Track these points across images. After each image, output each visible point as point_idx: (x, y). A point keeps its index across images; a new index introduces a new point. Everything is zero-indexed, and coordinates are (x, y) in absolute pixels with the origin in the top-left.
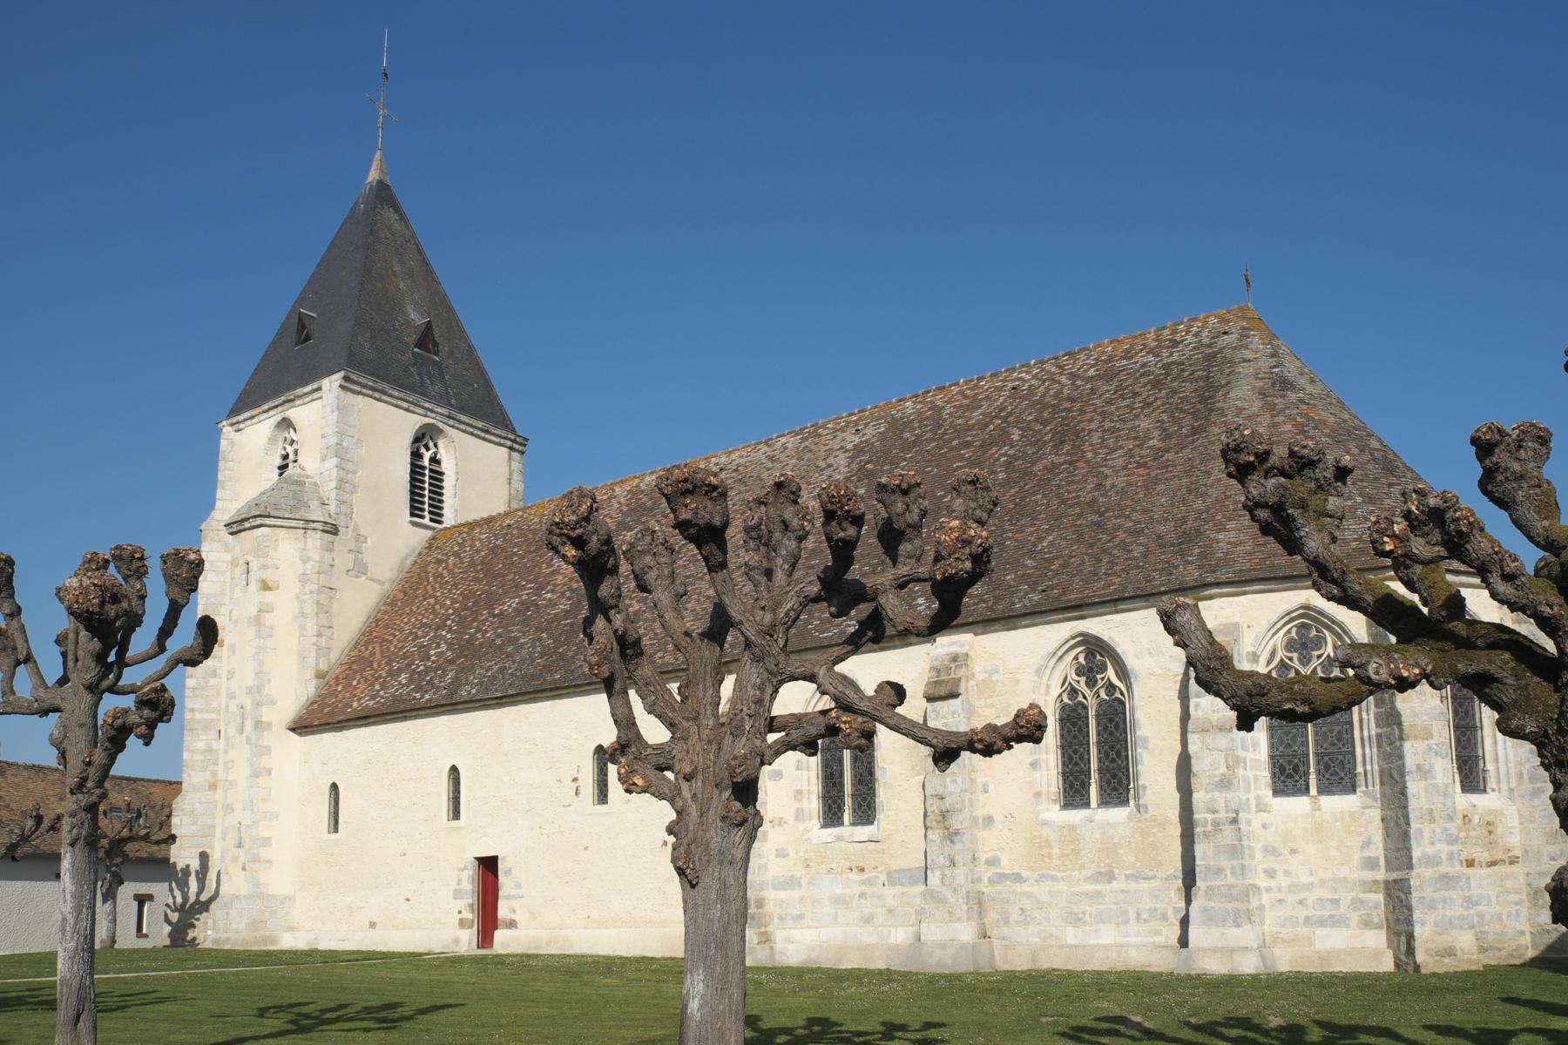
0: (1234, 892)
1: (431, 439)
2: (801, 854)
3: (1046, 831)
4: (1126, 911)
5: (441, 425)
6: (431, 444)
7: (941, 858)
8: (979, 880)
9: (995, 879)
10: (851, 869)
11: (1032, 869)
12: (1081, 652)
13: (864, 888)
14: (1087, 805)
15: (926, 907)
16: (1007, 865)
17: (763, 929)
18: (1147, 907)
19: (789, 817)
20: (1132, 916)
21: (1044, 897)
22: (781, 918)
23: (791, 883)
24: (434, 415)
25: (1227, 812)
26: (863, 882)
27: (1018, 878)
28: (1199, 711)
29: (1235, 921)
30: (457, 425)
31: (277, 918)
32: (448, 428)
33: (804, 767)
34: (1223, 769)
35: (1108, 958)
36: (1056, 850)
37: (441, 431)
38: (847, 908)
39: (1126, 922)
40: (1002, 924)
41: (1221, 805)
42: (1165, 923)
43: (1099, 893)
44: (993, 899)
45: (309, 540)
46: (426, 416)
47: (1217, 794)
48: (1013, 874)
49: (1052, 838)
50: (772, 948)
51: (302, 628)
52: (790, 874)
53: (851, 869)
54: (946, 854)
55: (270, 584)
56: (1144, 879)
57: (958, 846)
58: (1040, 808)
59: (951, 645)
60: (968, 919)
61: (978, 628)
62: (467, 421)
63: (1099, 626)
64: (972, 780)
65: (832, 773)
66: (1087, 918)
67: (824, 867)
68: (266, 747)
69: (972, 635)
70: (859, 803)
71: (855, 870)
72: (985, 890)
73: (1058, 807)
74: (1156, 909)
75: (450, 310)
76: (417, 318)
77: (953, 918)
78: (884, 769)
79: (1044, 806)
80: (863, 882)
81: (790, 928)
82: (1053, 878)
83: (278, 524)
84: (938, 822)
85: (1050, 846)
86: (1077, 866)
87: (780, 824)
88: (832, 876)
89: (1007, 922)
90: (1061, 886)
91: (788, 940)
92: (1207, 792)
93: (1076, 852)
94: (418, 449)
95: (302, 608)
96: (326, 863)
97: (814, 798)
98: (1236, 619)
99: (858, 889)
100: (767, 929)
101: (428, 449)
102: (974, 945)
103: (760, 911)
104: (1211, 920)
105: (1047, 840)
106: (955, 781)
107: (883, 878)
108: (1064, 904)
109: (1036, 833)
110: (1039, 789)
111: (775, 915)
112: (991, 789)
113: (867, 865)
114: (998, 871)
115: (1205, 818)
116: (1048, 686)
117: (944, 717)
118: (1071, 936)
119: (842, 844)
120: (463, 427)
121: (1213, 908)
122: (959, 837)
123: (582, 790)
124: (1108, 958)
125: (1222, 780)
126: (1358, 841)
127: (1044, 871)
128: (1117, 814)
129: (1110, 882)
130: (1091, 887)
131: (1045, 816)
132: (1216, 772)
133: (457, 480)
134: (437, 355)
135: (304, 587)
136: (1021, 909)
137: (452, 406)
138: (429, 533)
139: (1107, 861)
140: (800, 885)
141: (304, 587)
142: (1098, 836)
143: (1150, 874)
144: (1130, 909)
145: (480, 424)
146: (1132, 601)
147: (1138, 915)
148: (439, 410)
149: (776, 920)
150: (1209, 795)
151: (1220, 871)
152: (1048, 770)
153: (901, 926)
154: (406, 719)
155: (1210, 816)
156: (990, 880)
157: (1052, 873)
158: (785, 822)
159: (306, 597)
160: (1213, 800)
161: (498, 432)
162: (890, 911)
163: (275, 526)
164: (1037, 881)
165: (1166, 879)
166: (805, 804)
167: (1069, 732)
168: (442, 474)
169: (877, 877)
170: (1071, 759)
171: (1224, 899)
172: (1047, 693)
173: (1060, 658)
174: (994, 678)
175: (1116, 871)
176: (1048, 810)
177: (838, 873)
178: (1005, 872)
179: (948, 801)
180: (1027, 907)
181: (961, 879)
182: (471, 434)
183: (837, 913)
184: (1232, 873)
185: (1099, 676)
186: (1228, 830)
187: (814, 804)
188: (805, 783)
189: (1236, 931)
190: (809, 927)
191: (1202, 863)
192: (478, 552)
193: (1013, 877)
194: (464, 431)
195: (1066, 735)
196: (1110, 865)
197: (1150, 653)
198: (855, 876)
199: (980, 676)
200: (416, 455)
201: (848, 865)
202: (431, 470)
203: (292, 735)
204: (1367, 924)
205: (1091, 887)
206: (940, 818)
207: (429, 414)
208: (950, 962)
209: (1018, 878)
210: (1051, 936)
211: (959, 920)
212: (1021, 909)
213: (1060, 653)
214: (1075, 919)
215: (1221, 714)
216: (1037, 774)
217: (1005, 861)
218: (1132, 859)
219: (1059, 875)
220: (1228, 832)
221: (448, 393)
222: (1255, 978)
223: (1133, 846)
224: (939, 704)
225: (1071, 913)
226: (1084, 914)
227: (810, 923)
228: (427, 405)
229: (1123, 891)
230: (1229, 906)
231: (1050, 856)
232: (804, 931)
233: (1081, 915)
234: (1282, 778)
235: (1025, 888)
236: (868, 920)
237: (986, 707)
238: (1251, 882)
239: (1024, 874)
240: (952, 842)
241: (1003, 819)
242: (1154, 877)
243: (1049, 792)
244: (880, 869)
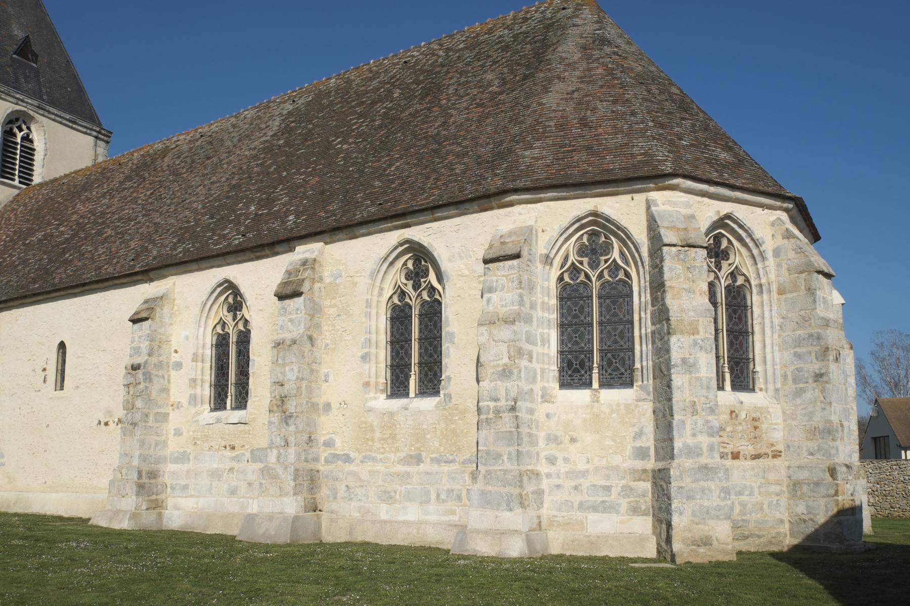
0: (509, 477)
1: (25, 123)
2: (191, 433)
3: (372, 418)
4: (429, 491)
5: (31, 113)
6: (24, 127)
7: (278, 439)
8: (316, 460)
9: (330, 459)
10: (225, 447)
11: (358, 450)
12: (409, 258)
13: (234, 464)
14: (407, 395)
15: (264, 482)
16: (340, 446)
17: (154, 497)
18: (445, 488)
19: (184, 401)
20: (433, 496)
21: (365, 476)
22: (173, 488)
23: (182, 458)
24: (25, 105)
25: (507, 400)
26: (233, 459)
27: (347, 459)
28: (490, 306)
29: (508, 505)
30: (46, 114)
32: (38, 116)
33: (200, 359)
34: (505, 360)
35: (409, 534)
36: (377, 435)
37: (32, 118)
38: (219, 480)
39: (428, 501)
40: (331, 499)
41: (502, 394)
42: (459, 504)
43: (408, 474)
44: (327, 477)
46: (17, 104)
47: (499, 383)
48: (344, 455)
49: (375, 424)
50: (160, 514)
52: (182, 450)
53: (225, 447)
54: (282, 435)
56: (446, 462)
57: (292, 428)
58: (367, 396)
59: (305, 252)
60: (295, 494)
61: (326, 237)
62: (56, 112)
63: (419, 233)
64: (312, 371)
65: (222, 365)
66: (397, 497)
69: (322, 244)
70: (219, 392)
71: (228, 448)
72: (321, 468)
73: (384, 396)
74: (452, 491)
75: (54, 34)
76: (19, 33)
77: (282, 493)
78: (254, 360)
79: (372, 395)
80: (233, 459)
81: (178, 497)
82: (374, 459)
84: (278, 406)
85: (373, 431)
86: (393, 449)
87: (178, 408)
88: (211, 452)
89: (335, 498)
90: (380, 467)
91: (176, 508)
92: (491, 381)
93: (393, 437)
94: (11, 129)
97: (207, 386)
98: (531, 223)
99: (228, 464)
100: (159, 497)
101: (21, 130)
102: (296, 519)
103: (152, 481)
104: (488, 503)
105: (371, 426)
106: (292, 369)
107: (248, 455)
108: (380, 483)
109: (363, 419)
110: (367, 380)
111: (169, 486)
112: (331, 378)
113: (237, 443)
114: (333, 452)
115: (488, 406)
116: (381, 289)
118: (384, 512)
119: (220, 425)
120: (53, 117)
121: (490, 492)
122: (292, 420)
123: (48, 379)
124: (409, 534)
125: (504, 370)
126: (631, 432)
127: (368, 453)
128: (429, 403)
129: (418, 465)
130: (402, 469)
131: (372, 404)
132: (500, 362)
133: (45, 155)
134: (36, 63)
136: (347, 486)
137: (44, 100)
138: (17, 192)
139: (416, 446)
140: (189, 460)
142: (410, 422)
143: (451, 458)
144: (431, 489)
145: (68, 116)
147: (438, 495)
148: (30, 101)
149: (169, 489)
150: (493, 384)
151: (498, 456)
152: (377, 363)
155: (492, 404)
156: (327, 461)
157: (373, 455)
158: (182, 406)
160: (496, 389)
161: (84, 124)
162: (250, 484)
164: (362, 462)
165: (463, 463)
166: (198, 391)
167: (398, 329)
168: (34, 150)
169: (243, 454)
170: (398, 353)
171: (500, 484)
172: (380, 294)
173: (392, 264)
174: (338, 281)
175: (424, 454)
176: (375, 398)
177: (215, 451)
178: (338, 452)
179: (287, 387)
180: (351, 484)
181: (292, 458)
182: (60, 123)
183: (211, 485)
184: (508, 458)
185: (422, 280)
186: (507, 417)
187: (206, 391)
188: (199, 372)
189: (508, 514)
190: (191, 496)
191: (484, 448)
192: (38, 202)
193: (343, 457)
194: (54, 120)
195: (395, 333)
196: (418, 449)
197: (460, 257)
198: (228, 453)
199: (328, 280)
200: (9, 133)
201: (223, 443)
202: (22, 146)
204: (635, 510)
205: (402, 469)
206: (279, 403)
207: (20, 103)
208: (273, 533)
209: (347, 459)
210: (369, 512)
211: (287, 494)
212: (347, 486)
213: (390, 259)
214: (387, 497)
215: (509, 308)
216: (367, 366)
217: (338, 443)
218: (437, 444)
219: (379, 456)
220: (507, 419)
221: (40, 90)
222: (520, 561)
223: (439, 432)
224: (287, 302)
225: (385, 492)
226: (395, 492)
227: (192, 493)
228: (18, 96)
229: (427, 473)
230: (504, 490)
231: (373, 440)
232: (187, 499)
233: (393, 494)
234: (570, 372)
235: (353, 467)
236: (233, 492)
237: (331, 306)
238: (530, 467)
239: (352, 455)
240: (287, 424)
241: (338, 405)
242: (453, 461)
243: (377, 383)
244: (246, 447)
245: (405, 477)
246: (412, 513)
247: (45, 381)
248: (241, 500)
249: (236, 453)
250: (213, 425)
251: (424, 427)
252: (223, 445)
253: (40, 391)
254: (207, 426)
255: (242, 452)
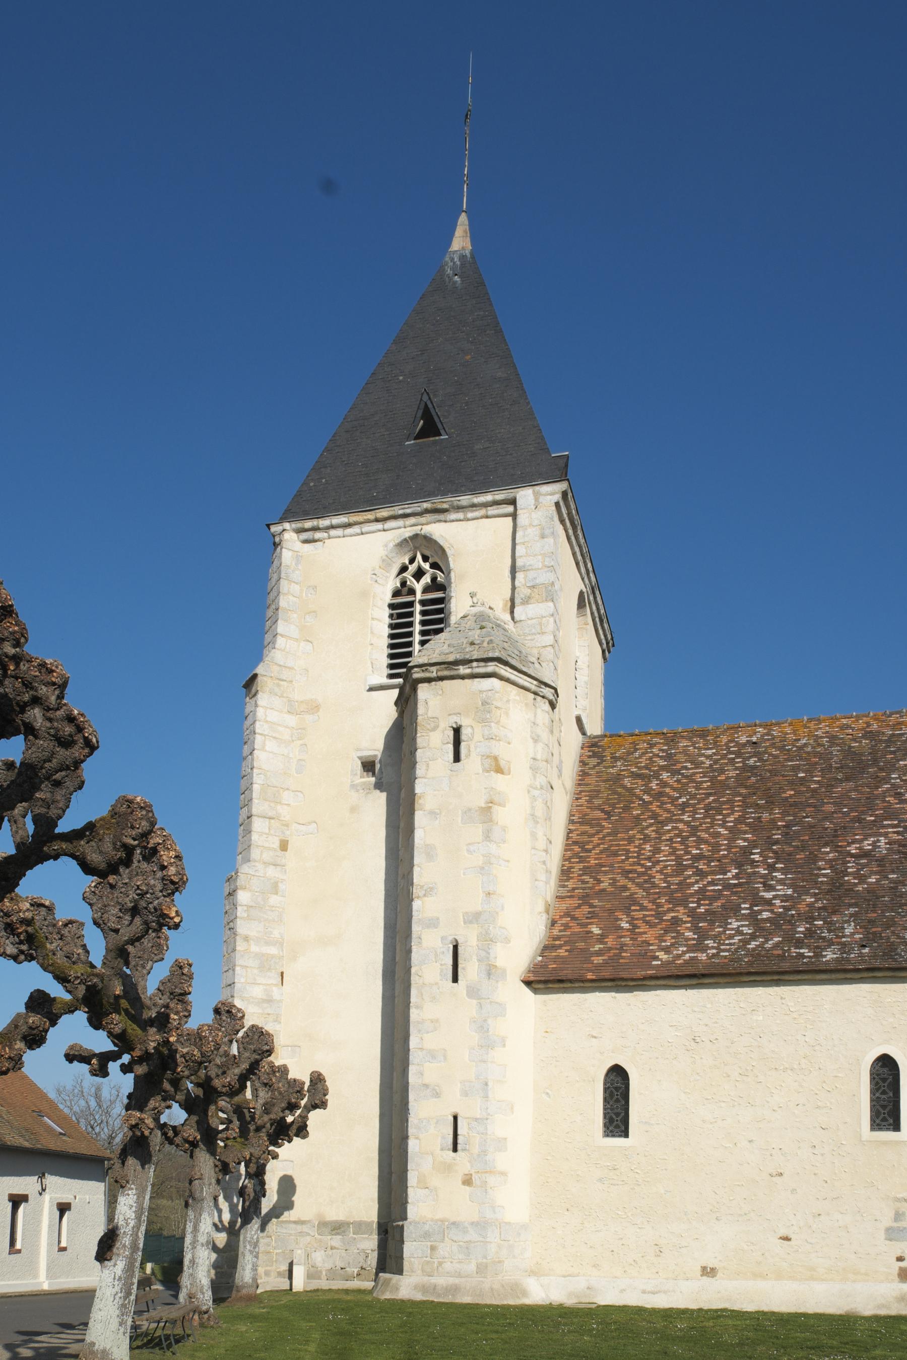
31: (514, 1257)
45: (539, 711)
51: (534, 835)
55: (502, 763)
68: (500, 1004)
83: (513, 677)
95: (533, 808)
96: (600, 1180)
135: (535, 777)
141: (535, 777)
154: (778, 983)
159: (536, 793)
163: (508, 680)
203: (523, 985)
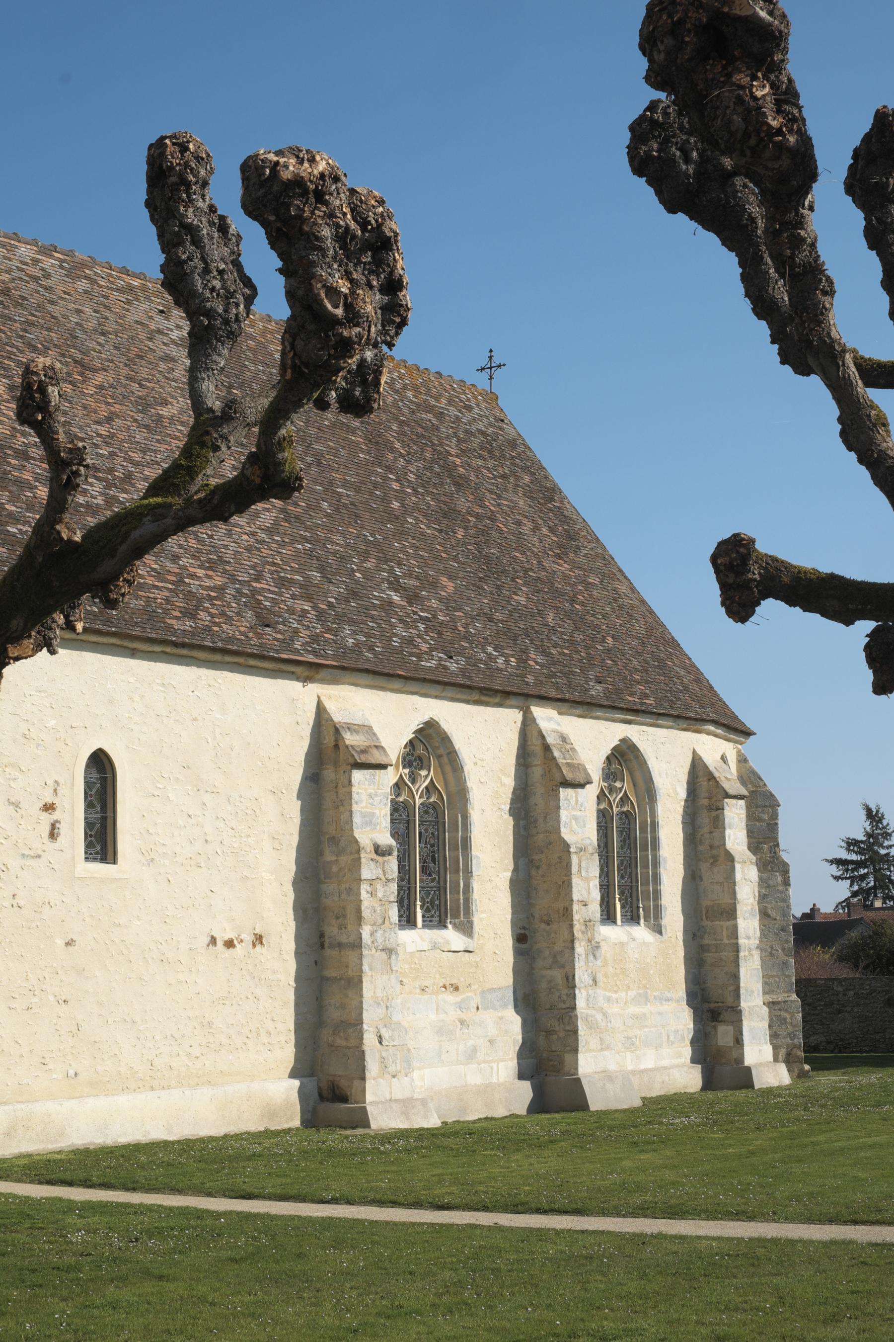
10: (445, 987)
20: (665, 1039)
39: (661, 1046)
42: (683, 1044)
54: (590, 971)
61: (565, 707)
67: (417, 984)
69: (555, 712)
78: (478, 858)
84: (583, 933)
88: (426, 997)
99: (453, 1014)
117: (573, 809)
130: (633, 1010)
142: (636, 956)
143: (669, 995)
146: (624, 712)
147: (668, 1037)
153: (503, 1061)
155: (746, 941)
162: (491, 1042)
197: (667, 774)
198: (450, 998)
205: (633, 1010)
206: (583, 928)
219: (614, 996)
225: (629, 1038)
229: (660, 1014)
233: (634, 1040)
236: (471, 1055)
245: (640, 1018)
246: (648, 1061)
247: (53, 834)
248: (482, 1065)
249: (461, 997)
250: (427, 953)
251: (648, 961)
252: (441, 985)
253: (39, 856)
254: (417, 954)
255: (470, 994)
